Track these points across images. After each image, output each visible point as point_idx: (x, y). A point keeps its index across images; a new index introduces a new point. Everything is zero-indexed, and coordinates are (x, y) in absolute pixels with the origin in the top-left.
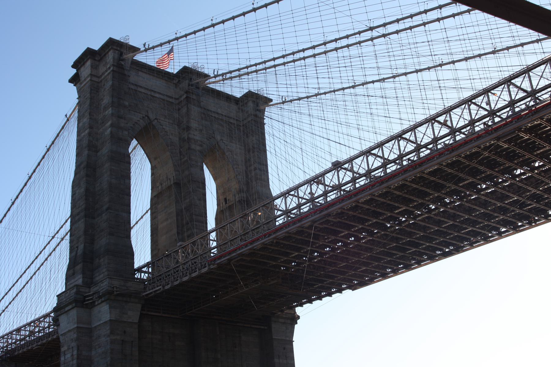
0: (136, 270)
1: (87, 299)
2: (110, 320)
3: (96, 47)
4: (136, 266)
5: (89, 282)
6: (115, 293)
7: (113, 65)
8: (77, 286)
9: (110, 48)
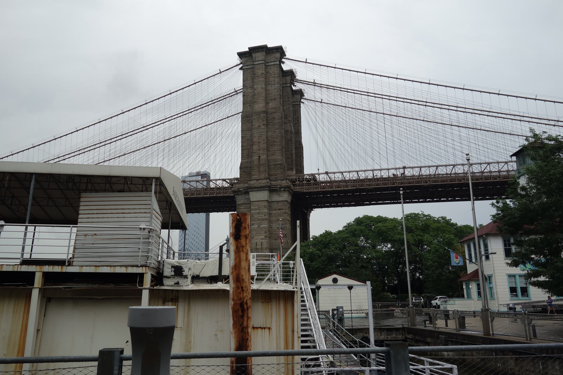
3: (269, 46)
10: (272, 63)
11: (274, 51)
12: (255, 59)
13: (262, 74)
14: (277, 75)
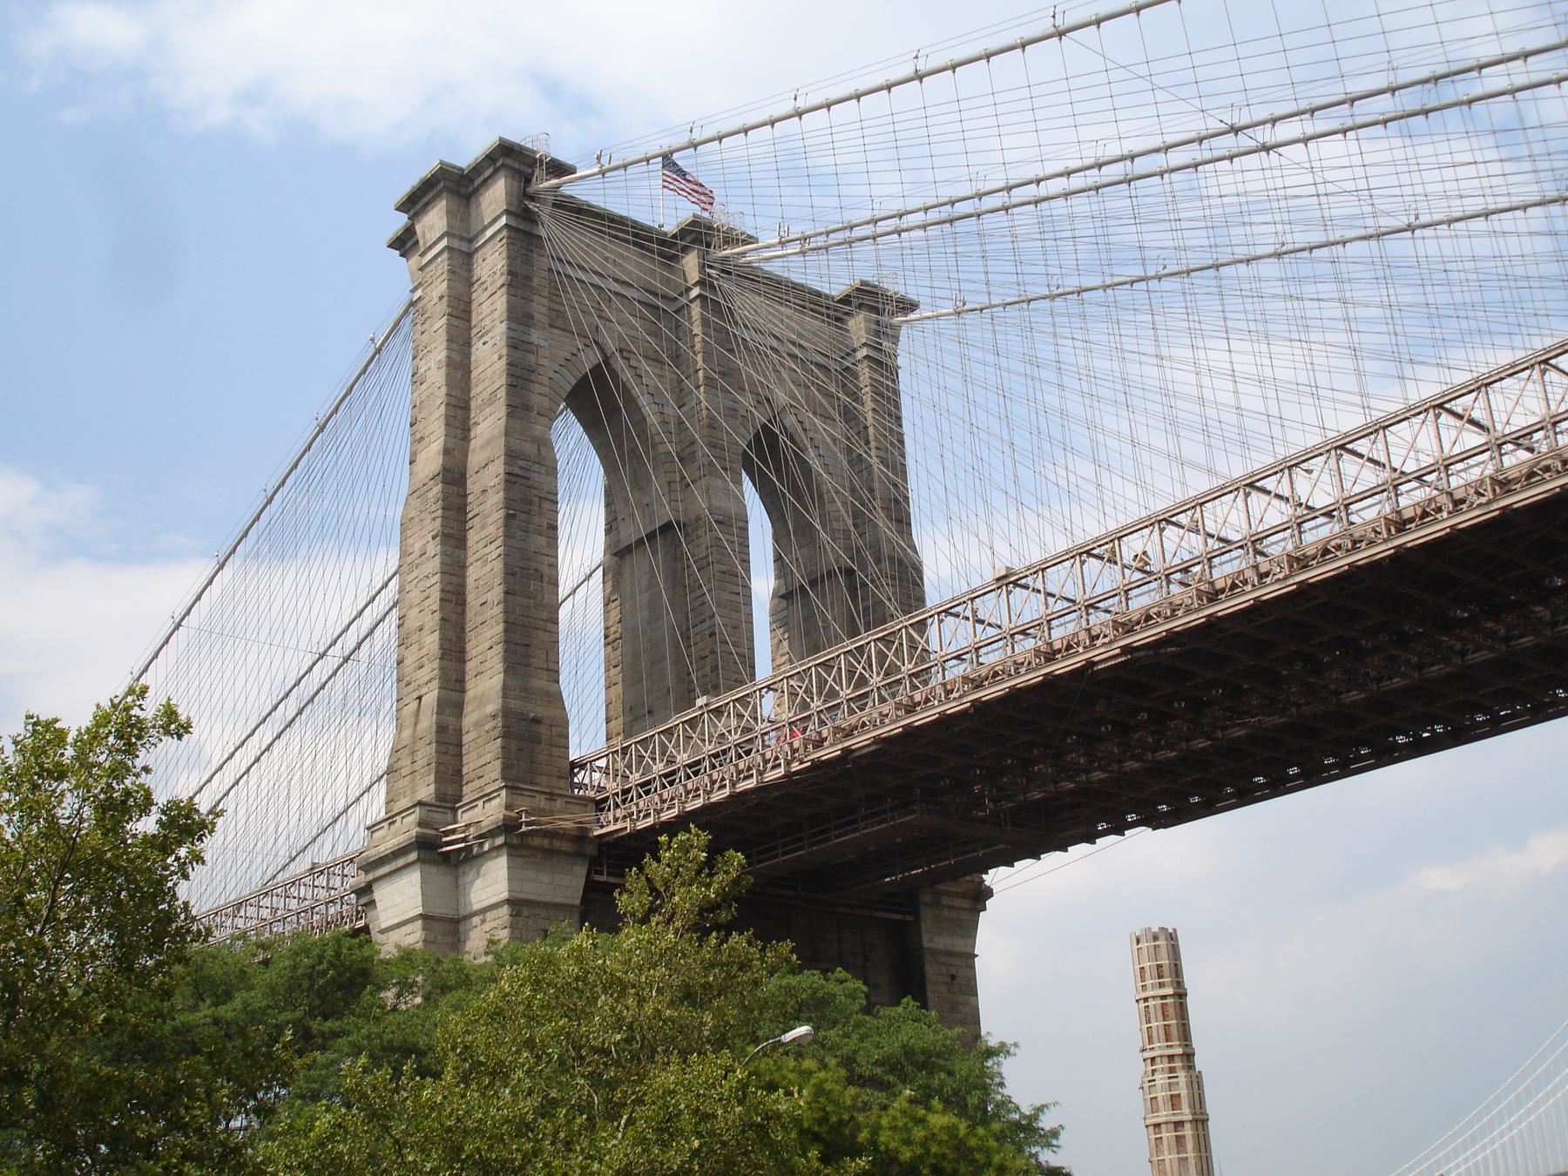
0: (573, 765)
1: (444, 839)
2: (508, 901)
4: (574, 755)
5: (449, 797)
6: (524, 829)
7: (508, 212)
8: (420, 803)
9: (499, 163)
10: (489, 233)
11: (487, 173)
12: (425, 243)
13: (441, 298)
14: (499, 283)
